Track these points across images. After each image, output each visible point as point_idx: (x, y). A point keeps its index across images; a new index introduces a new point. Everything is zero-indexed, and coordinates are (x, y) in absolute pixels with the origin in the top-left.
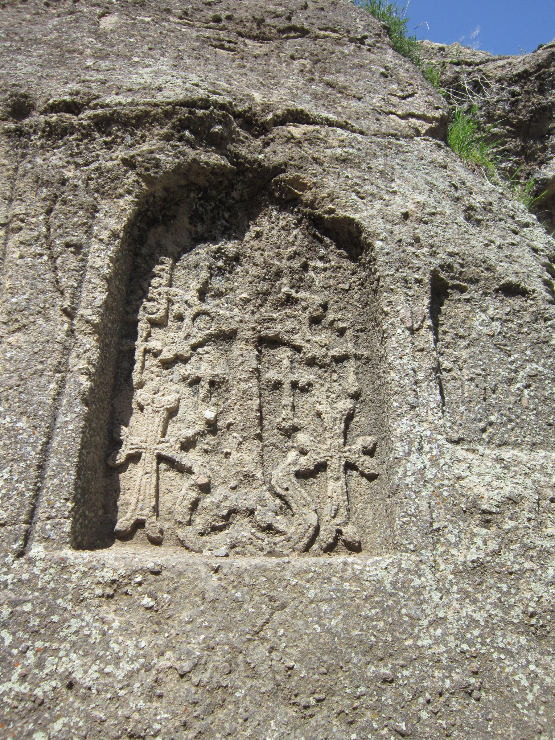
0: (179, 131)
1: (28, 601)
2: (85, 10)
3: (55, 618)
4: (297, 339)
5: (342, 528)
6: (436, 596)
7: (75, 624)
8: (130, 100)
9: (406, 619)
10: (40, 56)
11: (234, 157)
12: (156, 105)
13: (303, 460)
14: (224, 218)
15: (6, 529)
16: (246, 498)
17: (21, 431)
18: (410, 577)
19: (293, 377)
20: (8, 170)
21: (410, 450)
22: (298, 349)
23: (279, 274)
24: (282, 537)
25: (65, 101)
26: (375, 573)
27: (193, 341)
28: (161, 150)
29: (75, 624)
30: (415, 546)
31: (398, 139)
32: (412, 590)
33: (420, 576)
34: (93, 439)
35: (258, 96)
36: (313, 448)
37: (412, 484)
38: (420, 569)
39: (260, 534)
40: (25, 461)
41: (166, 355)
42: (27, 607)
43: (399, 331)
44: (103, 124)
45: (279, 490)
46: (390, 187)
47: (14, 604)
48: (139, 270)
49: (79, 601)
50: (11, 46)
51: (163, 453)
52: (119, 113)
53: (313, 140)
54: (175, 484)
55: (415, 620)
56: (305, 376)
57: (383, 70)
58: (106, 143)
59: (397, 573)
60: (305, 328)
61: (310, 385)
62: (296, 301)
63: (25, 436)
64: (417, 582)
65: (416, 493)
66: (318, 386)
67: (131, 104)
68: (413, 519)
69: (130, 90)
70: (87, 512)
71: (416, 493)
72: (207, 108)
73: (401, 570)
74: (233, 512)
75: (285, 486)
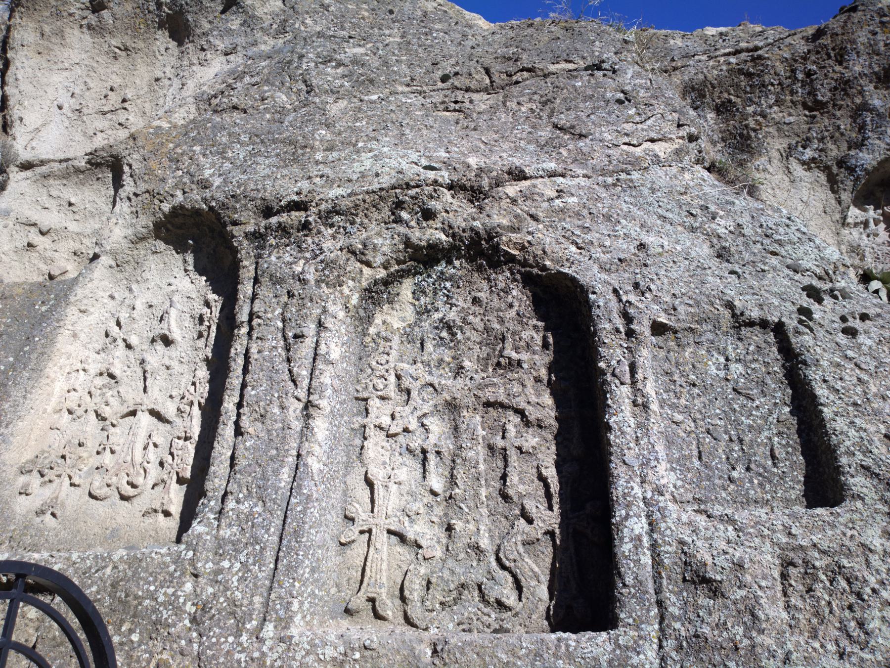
2: (318, 101)
8: (349, 191)
10: (277, 155)
11: (449, 229)
14: (445, 288)
18: (630, 654)
21: (627, 514)
22: (520, 412)
24: (509, 613)
25: (293, 201)
26: (590, 650)
27: (420, 413)
28: (379, 234)
30: (634, 620)
31: (630, 174)
33: (638, 653)
34: (323, 519)
35: (473, 161)
36: (539, 515)
37: (630, 551)
38: (639, 646)
44: (326, 217)
45: (507, 563)
46: (614, 231)
48: (367, 349)
50: (253, 149)
51: (393, 528)
53: (527, 196)
54: (403, 558)
57: (621, 96)
60: (530, 390)
62: (519, 363)
63: (260, 520)
65: (635, 561)
66: (543, 448)
67: (349, 195)
68: (633, 590)
69: (350, 181)
70: (317, 592)
71: (635, 561)
72: (418, 186)
73: (619, 646)
75: (511, 557)
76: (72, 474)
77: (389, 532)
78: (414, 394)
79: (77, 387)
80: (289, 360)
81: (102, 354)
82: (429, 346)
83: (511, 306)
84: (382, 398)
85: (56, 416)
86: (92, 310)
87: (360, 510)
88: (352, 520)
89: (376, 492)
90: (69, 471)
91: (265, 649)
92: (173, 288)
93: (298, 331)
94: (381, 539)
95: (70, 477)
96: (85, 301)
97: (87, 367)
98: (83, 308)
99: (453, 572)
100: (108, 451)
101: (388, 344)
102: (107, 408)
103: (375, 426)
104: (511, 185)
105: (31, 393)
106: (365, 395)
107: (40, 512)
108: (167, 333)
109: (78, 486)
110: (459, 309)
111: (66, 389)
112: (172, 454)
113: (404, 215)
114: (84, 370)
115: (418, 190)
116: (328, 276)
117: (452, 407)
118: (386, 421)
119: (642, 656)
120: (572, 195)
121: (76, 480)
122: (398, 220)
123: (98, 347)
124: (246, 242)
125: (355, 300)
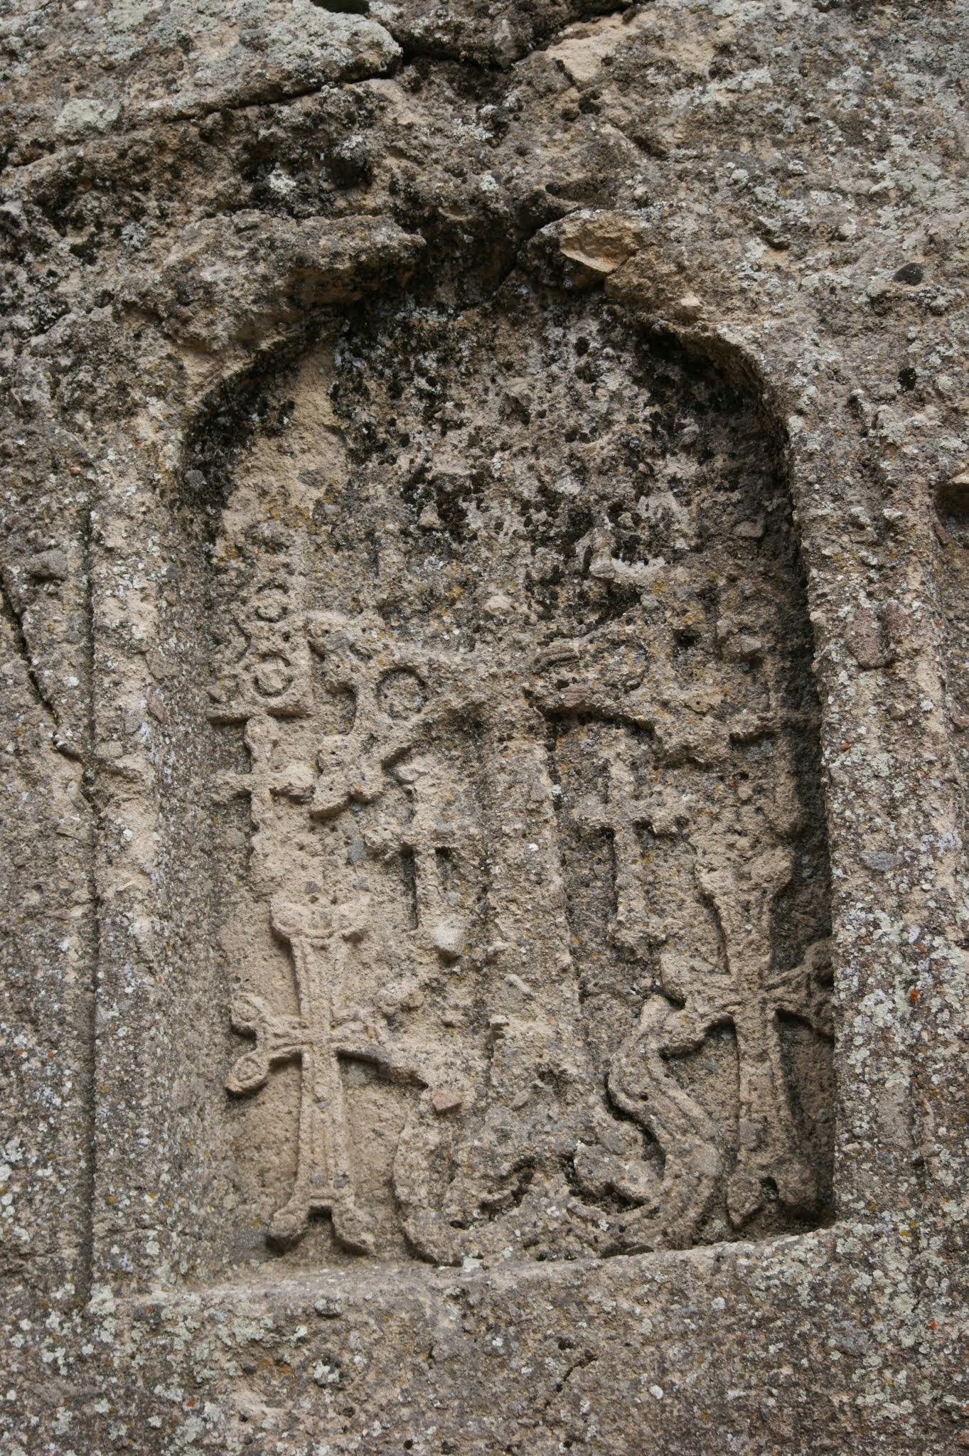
0: (248, 178)
1: (100, 1396)
3: (155, 1421)
4: (640, 705)
5: (775, 1175)
6: (904, 1305)
7: (192, 1427)
9: (836, 1356)
11: (413, 210)
12: (182, 117)
13: (674, 1020)
14: (422, 372)
15: (35, 1263)
16: (555, 1128)
17: (24, 1055)
18: (854, 1271)
19: (637, 810)
21: (863, 984)
22: (641, 730)
23: (582, 522)
24: (637, 1213)
26: (777, 1268)
27: (384, 751)
28: (215, 249)
29: (192, 1427)
30: (869, 1204)
32: (852, 1299)
33: (871, 1267)
34: (180, 1045)
36: (697, 986)
37: (864, 1065)
39: (585, 1210)
40: (45, 1118)
41: (325, 799)
42: (102, 1407)
43: (843, 677)
47: (75, 1402)
48: (224, 578)
49: (193, 1385)
51: (350, 1048)
52: (92, 164)
54: (386, 1115)
55: (853, 1358)
56: (671, 801)
58: (75, 250)
59: (826, 1267)
60: (663, 669)
61: (681, 822)
63: (35, 1063)
64: (863, 1280)
65: (873, 1084)
66: (703, 820)
67: (116, 126)
68: (867, 1145)
70: (194, 1209)
71: (873, 1084)
73: (835, 1258)
74: (526, 1167)
75: (637, 1089)
77: (345, 1058)
78: (365, 699)
80: (23, 646)
82: (392, 557)
83: (606, 422)
84: (282, 716)
87: (267, 1012)
88: (249, 1036)
89: (299, 963)
91: (106, 1337)
93: (35, 561)
94: (326, 1076)
99: (504, 1136)
101: (282, 558)
103: (274, 793)
104: (580, 35)
106: (238, 708)
110: (465, 433)
113: (281, 183)
115: (307, 103)
116: (90, 389)
117: (469, 724)
118: (298, 774)
119: (878, 1273)
120: (757, 60)
122: (263, 199)
125: (171, 456)
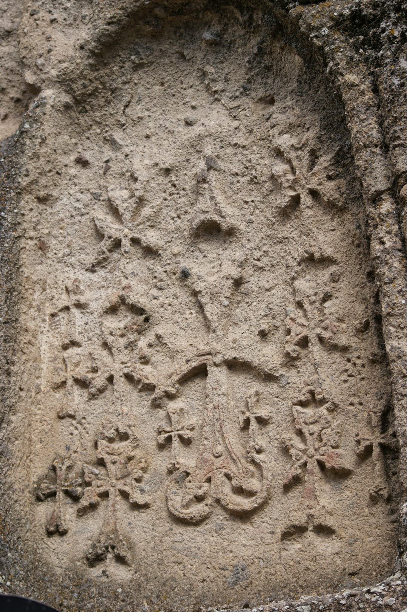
20: (363, 93)
76: (127, 489)
79: (78, 338)
81: (101, 273)
85: (59, 395)
86: (55, 193)
90: (120, 485)
92: (198, 130)
95: (125, 495)
96: (43, 181)
97: (83, 299)
98: (42, 194)
100: (176, 442)
102: (148, 369)
105: (13, 363)
107: (95, 559)
108: (216, 218)
109: (146, 506)
111: (58, 344)
112: (300, 433)
114: (79, 306)
121: (138, 497)
123: (90, 259)
124: (339, 38)
